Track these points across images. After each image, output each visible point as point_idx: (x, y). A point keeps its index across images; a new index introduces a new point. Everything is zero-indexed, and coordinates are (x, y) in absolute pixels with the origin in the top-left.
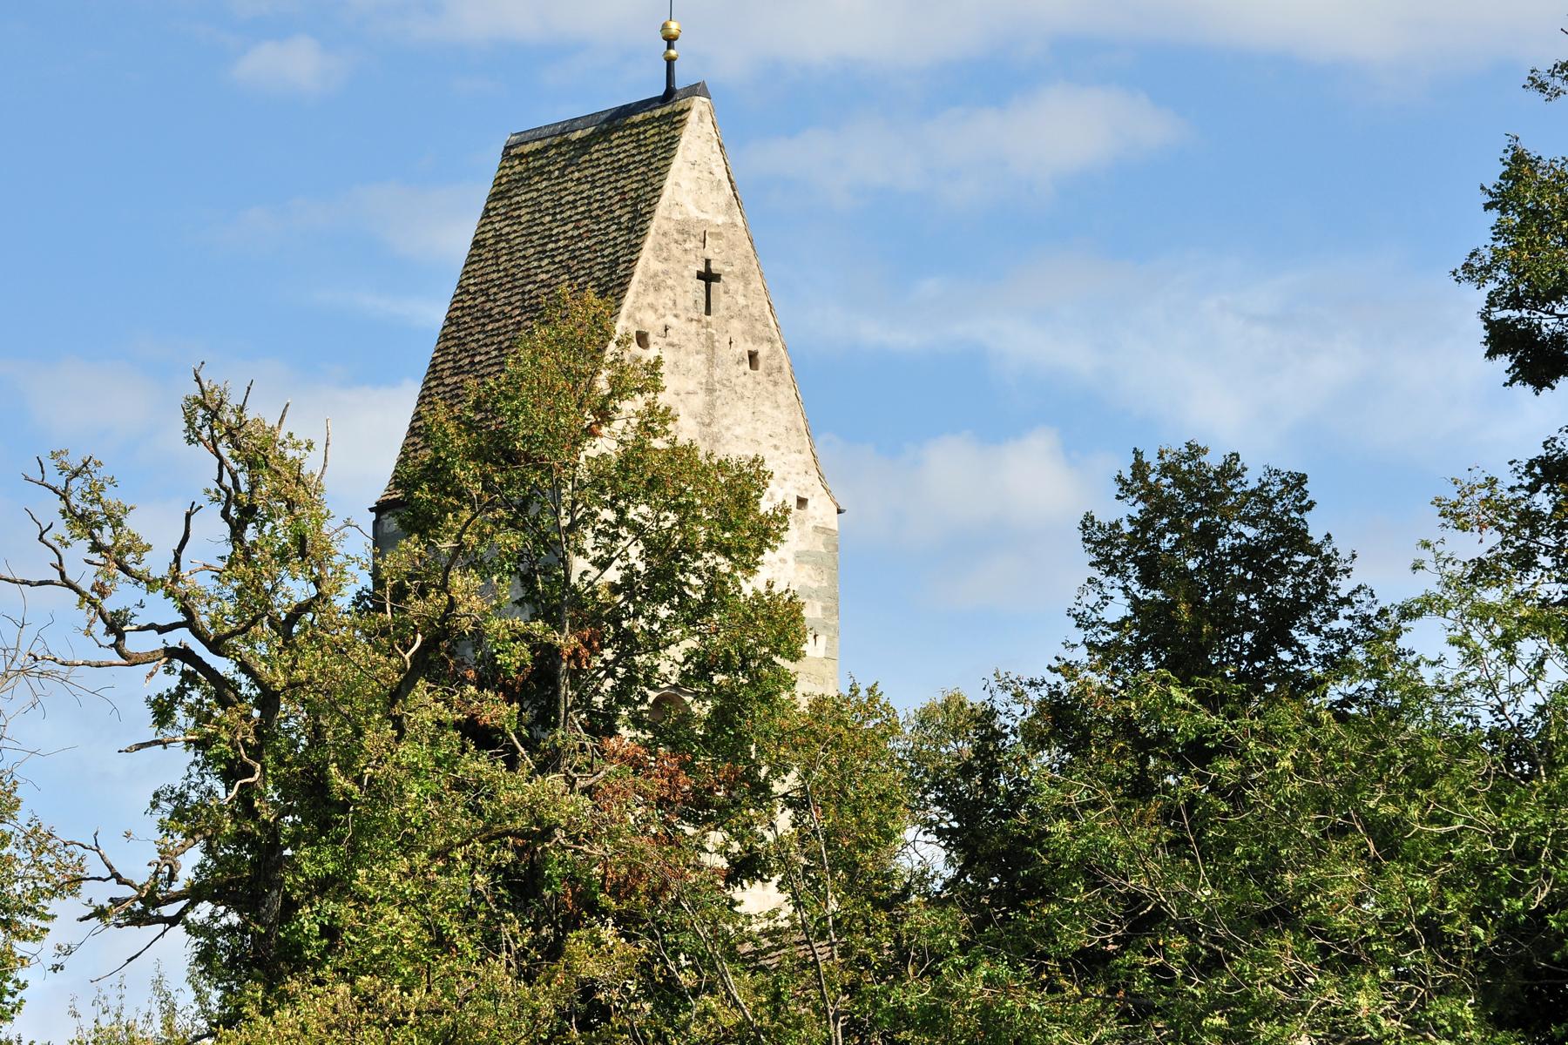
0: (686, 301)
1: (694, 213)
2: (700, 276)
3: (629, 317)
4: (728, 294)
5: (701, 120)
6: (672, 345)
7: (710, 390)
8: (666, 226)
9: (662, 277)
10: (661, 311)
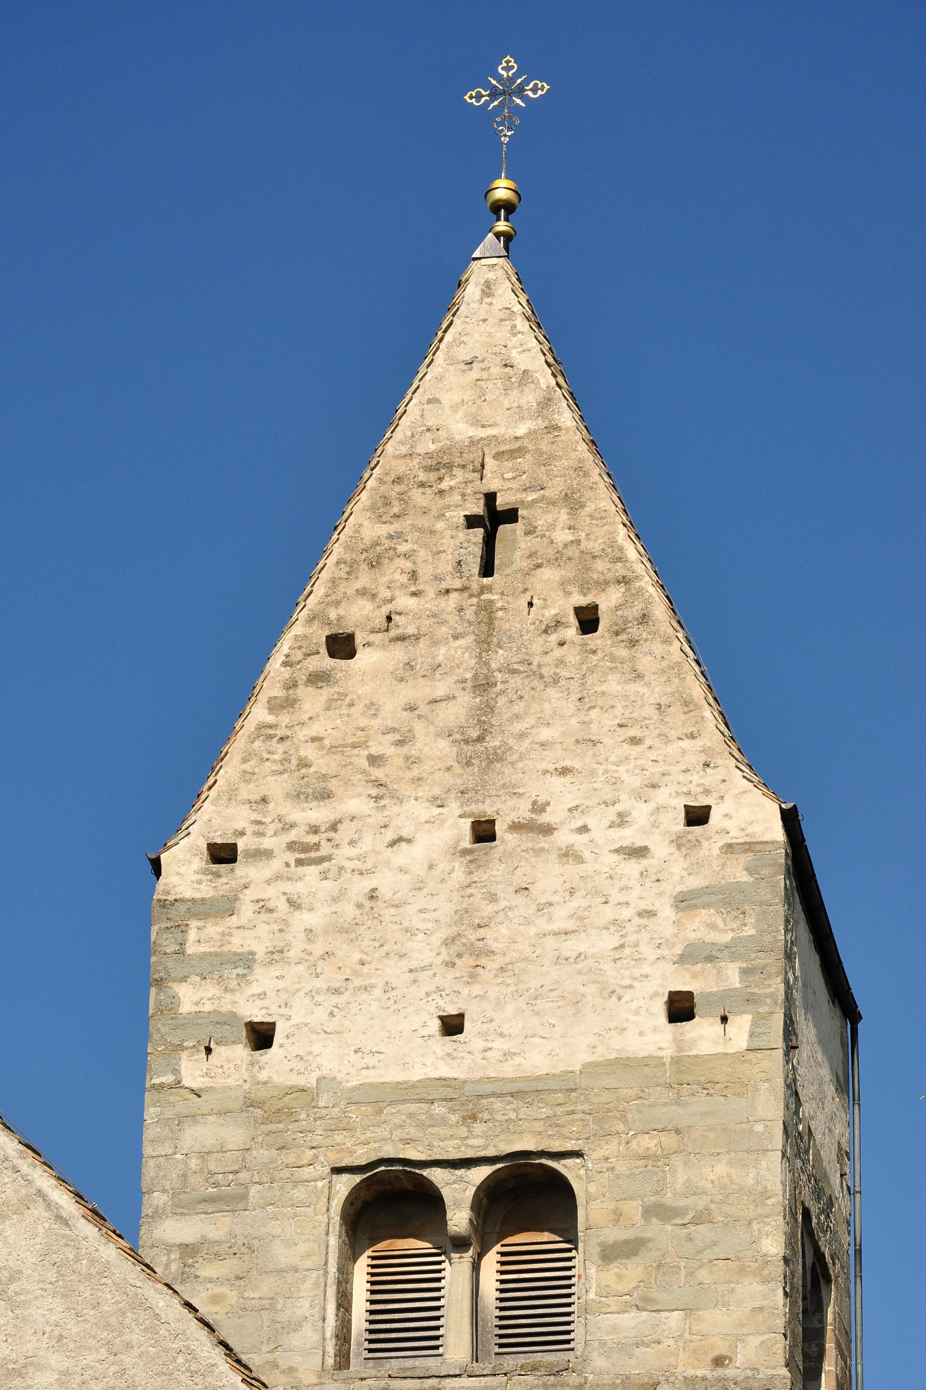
1: (462, 430)
2: (472, 522)
3: (311, 620)
6: (402, 638)
7: (483, 685)
8: (401, 467)
9: (387, 543)
10: (385, 593)
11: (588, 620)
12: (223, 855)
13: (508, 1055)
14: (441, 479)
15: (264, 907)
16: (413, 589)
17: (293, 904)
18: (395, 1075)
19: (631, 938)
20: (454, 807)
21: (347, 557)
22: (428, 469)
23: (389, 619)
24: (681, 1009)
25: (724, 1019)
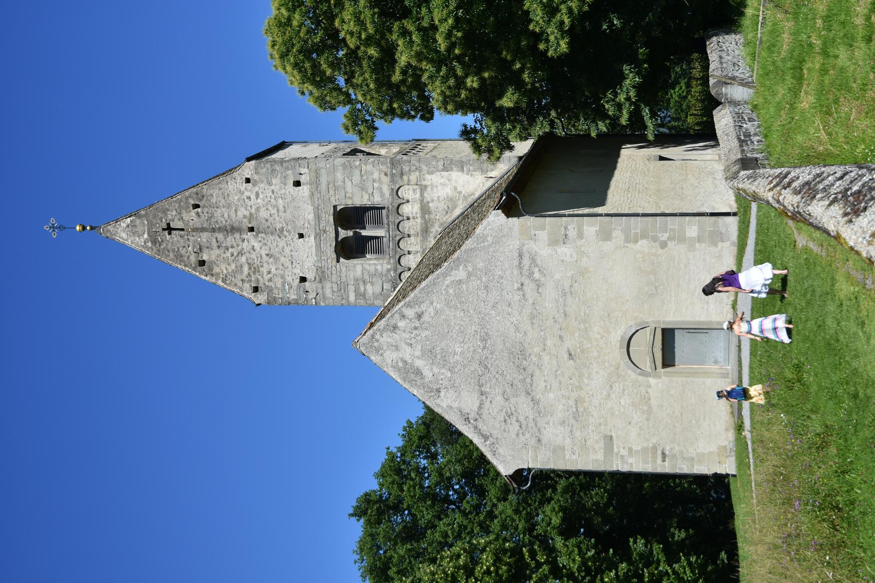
6: (200, 249)
7: (214, 230)
8: (155, 250)
11: (196, 206)
12: (256, 289)
13: (309, 223)
15: (270, 280)
17: (269, 272)
18: (314, 249)
20: (245, 236)
24: (297, 184)
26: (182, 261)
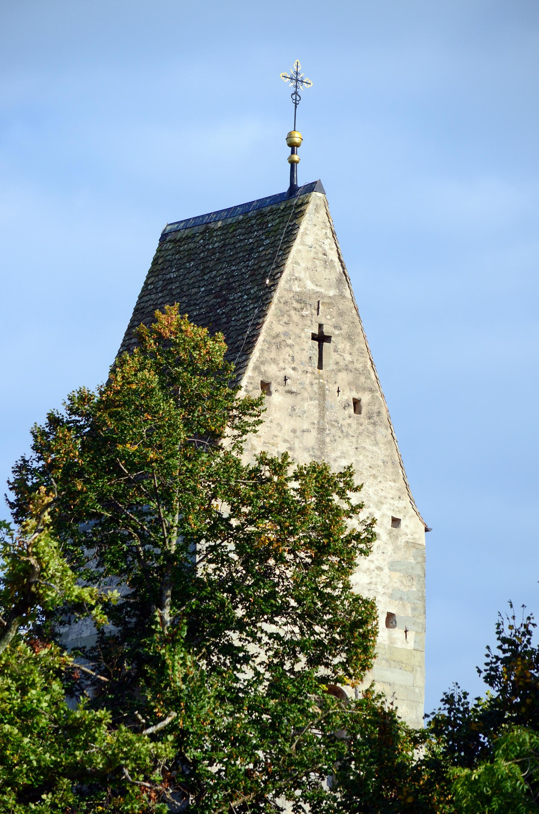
0: (304, 356)
1: (310, 286)
2: (314, 337)
3: (256, 368)
4: (337, 352)
5: (317, 210)
7: (321, 430)
10: (282, 365)
14: (302, 309)
16: (293, 366)
19: (374, 580)
21: (268, 339)
22: (298, 301)
23: (285, 380)
25: (406, 632)
26: (270, 343)
